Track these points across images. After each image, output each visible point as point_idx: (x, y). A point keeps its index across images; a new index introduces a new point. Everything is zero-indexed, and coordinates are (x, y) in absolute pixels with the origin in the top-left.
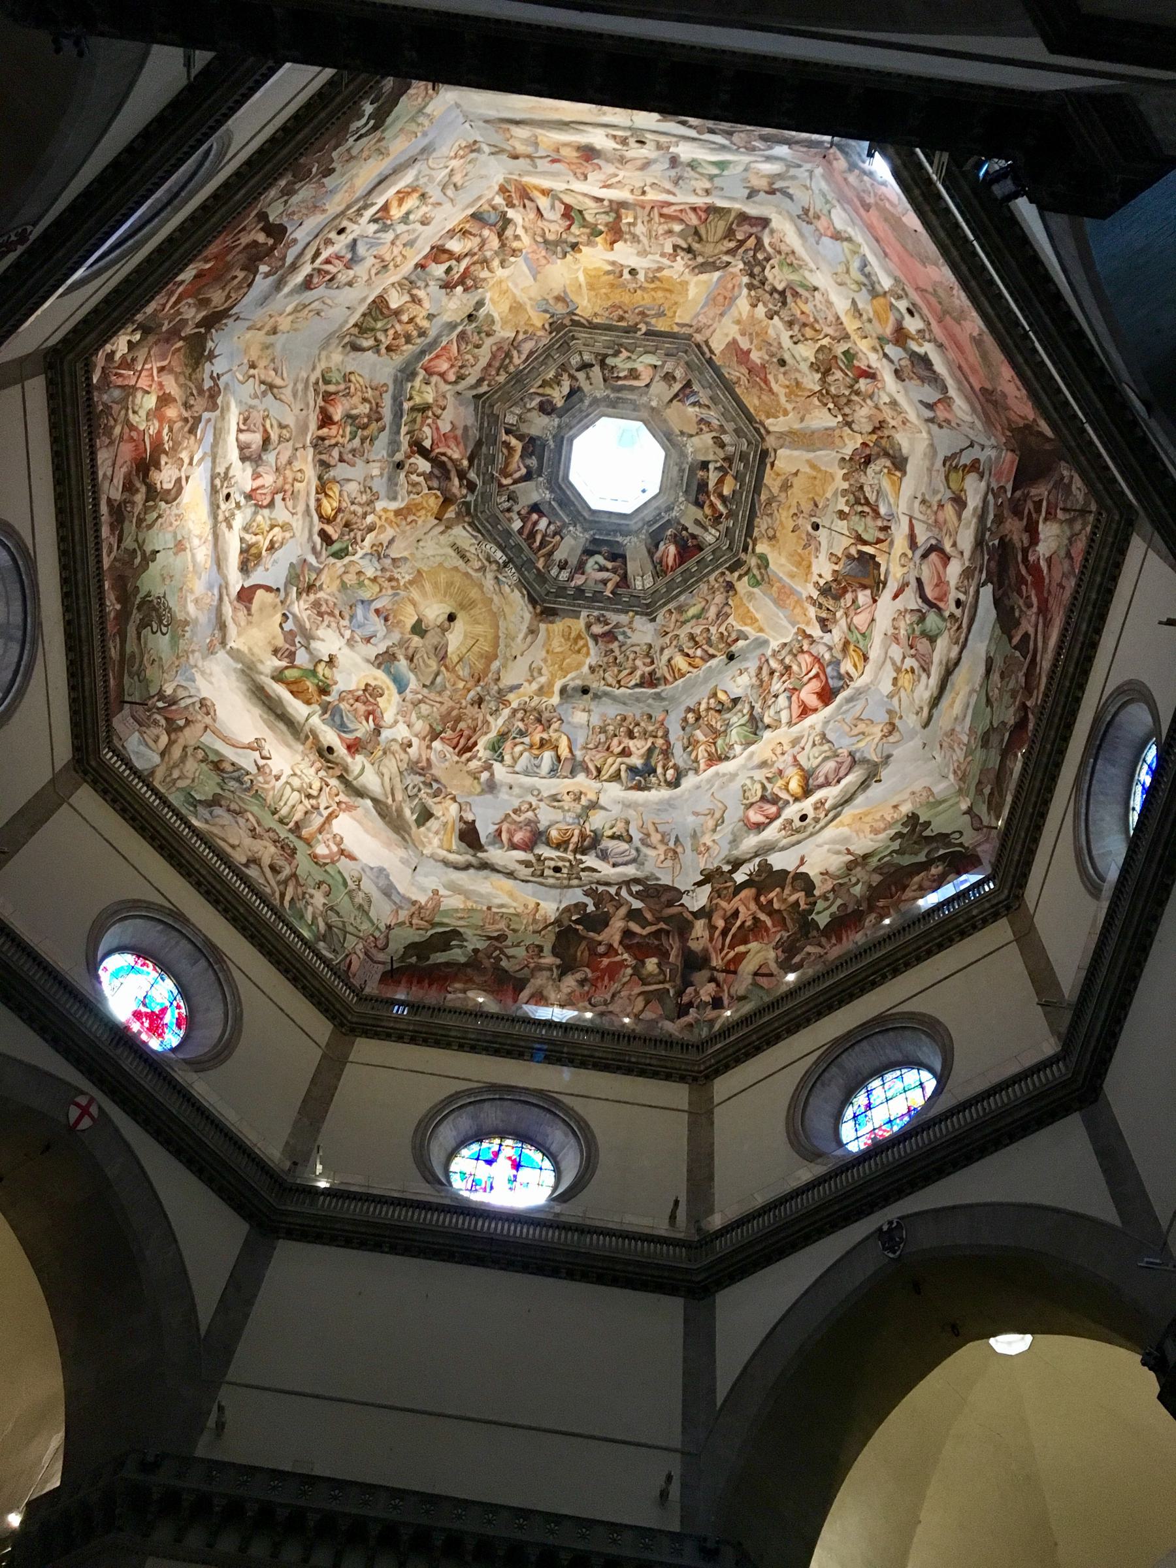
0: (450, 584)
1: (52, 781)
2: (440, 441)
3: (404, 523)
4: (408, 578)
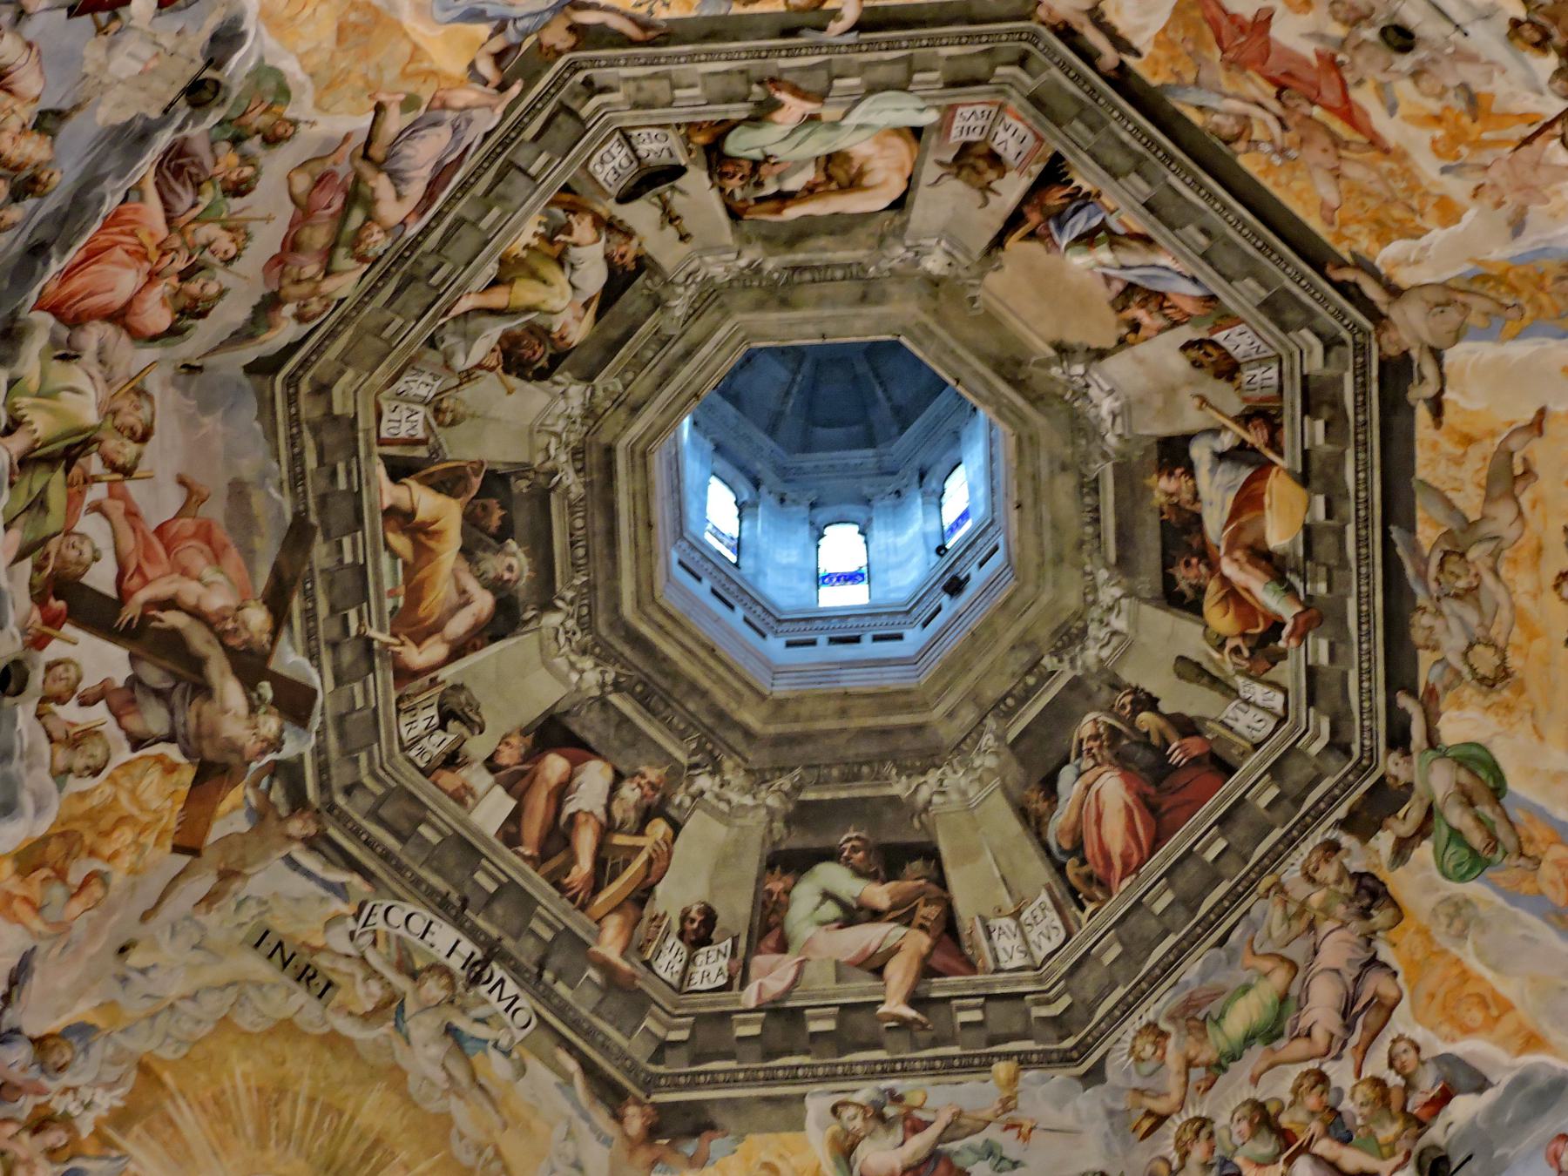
0: (273, 1095)
2: (149, 555)
3: (58, 892)
4: (106, 1101)
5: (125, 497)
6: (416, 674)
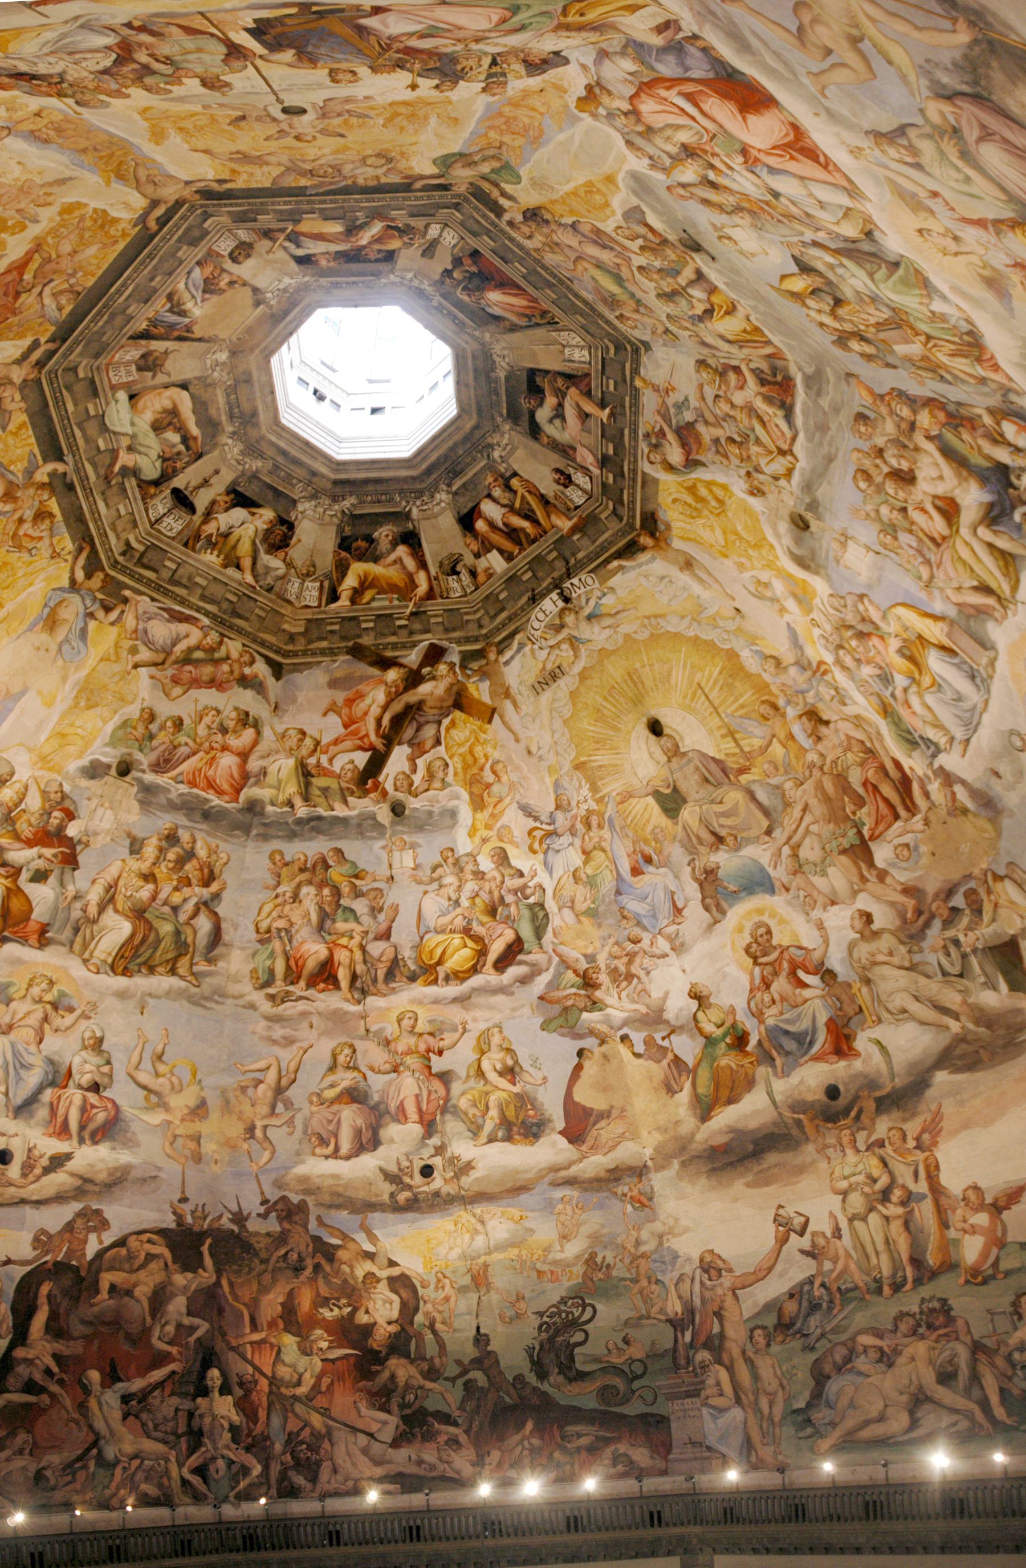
0: (599, 715)
3: (495, 788)
4: (585, 791)
5: (328, 745)
6: (431, 588)
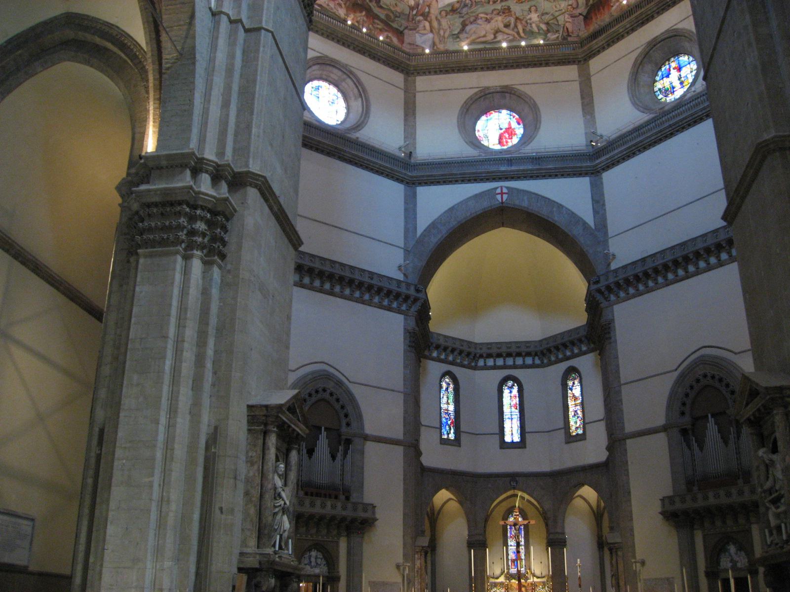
1: (405, 92)
